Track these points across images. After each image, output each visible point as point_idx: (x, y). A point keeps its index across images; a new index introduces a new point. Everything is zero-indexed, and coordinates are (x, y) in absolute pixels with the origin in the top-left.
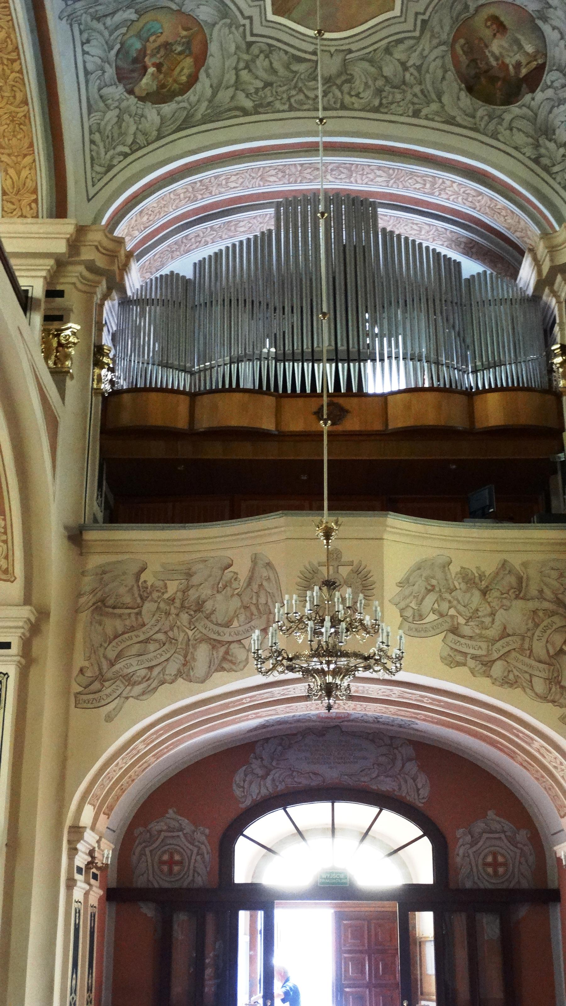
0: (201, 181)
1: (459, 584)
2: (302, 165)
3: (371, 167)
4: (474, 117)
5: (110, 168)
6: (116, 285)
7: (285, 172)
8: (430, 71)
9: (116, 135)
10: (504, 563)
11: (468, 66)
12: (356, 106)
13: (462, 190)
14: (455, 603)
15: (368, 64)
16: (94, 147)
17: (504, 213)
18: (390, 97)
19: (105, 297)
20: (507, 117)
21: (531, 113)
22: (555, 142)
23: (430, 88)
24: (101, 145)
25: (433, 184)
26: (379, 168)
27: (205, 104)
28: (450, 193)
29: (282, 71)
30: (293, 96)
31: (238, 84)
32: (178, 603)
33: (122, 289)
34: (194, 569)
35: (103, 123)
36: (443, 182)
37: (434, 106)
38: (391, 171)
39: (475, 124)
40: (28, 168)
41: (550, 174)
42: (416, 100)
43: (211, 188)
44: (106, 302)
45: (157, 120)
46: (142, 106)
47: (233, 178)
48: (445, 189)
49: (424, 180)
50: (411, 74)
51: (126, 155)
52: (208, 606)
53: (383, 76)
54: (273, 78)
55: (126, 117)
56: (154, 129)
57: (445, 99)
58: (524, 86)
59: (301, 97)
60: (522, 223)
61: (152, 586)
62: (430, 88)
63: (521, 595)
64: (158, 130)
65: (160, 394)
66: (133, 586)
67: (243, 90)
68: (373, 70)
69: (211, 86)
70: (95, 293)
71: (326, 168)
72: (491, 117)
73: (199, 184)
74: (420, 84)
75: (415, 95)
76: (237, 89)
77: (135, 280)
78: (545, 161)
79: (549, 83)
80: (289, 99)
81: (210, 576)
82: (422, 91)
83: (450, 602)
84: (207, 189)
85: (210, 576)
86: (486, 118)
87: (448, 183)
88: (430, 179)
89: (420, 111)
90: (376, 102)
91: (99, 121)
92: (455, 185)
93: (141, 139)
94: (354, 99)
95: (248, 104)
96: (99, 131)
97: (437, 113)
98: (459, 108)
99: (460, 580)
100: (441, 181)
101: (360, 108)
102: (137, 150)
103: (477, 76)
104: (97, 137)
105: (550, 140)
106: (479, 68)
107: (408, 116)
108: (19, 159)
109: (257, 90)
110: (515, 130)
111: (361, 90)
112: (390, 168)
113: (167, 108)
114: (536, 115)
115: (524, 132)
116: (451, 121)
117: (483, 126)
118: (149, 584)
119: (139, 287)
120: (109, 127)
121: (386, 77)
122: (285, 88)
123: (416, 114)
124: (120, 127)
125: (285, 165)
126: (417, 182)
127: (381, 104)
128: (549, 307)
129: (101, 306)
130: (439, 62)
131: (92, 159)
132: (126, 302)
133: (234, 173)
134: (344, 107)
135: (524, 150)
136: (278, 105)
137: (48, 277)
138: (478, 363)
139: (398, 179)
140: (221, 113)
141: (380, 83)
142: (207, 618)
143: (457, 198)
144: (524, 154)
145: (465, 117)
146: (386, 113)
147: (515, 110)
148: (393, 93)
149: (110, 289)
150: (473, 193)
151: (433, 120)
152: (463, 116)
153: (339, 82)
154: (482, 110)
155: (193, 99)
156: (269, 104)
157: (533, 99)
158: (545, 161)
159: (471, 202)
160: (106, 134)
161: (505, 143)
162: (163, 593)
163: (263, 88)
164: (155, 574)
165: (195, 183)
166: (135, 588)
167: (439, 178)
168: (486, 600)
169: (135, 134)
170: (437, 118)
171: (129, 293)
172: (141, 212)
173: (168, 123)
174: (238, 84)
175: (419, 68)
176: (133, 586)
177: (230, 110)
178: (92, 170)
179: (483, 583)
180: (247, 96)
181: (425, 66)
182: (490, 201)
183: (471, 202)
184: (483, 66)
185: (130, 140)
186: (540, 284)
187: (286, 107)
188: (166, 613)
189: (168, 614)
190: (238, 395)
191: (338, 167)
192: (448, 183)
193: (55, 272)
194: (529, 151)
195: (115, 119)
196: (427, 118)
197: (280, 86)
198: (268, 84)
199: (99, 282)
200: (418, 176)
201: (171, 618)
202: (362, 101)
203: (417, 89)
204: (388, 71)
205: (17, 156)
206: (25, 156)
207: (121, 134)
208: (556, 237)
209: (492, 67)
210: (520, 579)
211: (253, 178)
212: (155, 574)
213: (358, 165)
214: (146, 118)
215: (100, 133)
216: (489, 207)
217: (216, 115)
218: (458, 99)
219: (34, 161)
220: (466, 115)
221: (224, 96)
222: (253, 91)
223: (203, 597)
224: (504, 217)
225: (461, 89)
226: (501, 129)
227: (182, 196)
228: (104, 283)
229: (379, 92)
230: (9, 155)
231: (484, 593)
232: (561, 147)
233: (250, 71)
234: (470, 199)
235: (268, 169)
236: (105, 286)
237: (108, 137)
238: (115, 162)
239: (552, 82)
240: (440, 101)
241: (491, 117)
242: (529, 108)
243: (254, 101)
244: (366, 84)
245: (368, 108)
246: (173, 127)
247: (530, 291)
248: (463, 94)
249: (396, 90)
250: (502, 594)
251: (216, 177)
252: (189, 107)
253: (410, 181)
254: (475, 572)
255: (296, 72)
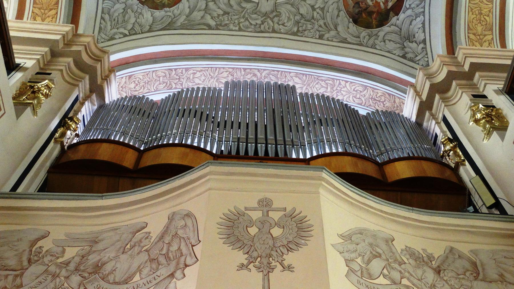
0: (176, 69)
1: (408, 259)
2: (245, 69)
3: (292, 74)
4: (359, 37)
5: (112, 39)
6: (97, 90)
7: (233, 76)
8: (330, 10)
9: (120, 20)
10: (452, 249)
11: (354, 7)
12: (282, 31)
13: (353, 88)
14: (407, 274)
15: (290, 6)
16: (102, 21)
17: (383, 99)
18: (304, 28)
19: (87, 98)
20: (381, 34)
21: (397, 28)
22: (416, 42)
23: (330, 23)
24: (109, 23)
25: (332, 88)
26: (297, 75)
27: (185, 17)
28: (344, 93)
29: (235, 7)
30: (241, 22)
31: (207, 9)
32: (72, 266)
33: (101, 96)
34: (100, 238)
35: (112, 10)
36: (340, 84)
37: (333, 33)
38: (304, 77)
39: (360, 41)
40: (51, 17)
41: (415, 62)
42: (320, 29)
43: (182, 80)
44: (86, 103)
45: (151, 19)
46: (142, 8)
47: (198, 74)
48: (341, 90)
49: (327, 84)
50: (318, 13)
51: (125, 35)
52: (108, 267)
53: (300, 13)
54: (228, 10)
55: (129, 11)
56: (148, 24)
57: (340, 28)
58: (391, 13)
59: (247, 23)
60: (397, 100)
61: (47, 251)
62: (330, 23)
63: (481, 277)
64: (150, 26)
65: (112, 146)
66: (24, 251)
67: (210, 14)
68: (293, 10)
69: (189, 7)
70: (78, 86)
71: (261, 74)
72: (370, 36)
73: (174, 72)
74: (324, 19)
75: (320, 26)
76: (206, 13)
77: (113, 93)
78: (409, 56)
79: (408, 6)
80: (239, 24)
81: (118, 241)
82: (325, 24)
83: (400, 272)
84: (179, 79)
85: (118, 241)
86: (367, 37)
87: (343, 83)
88: (330, 82)
89: (323, 35)
90: (295, 29)
91: (110, 8)
92: (348, 84)
93: (137, 28)
94: (281, 27)
95: (212, 23)
96: (109, 14)
97: (335, 37)
98: (349, 33)
99: (408, 256)
100: (338, 81)
101: (285, 32)
102: (134, 34)
103: (360, 13)
104: (107, 17)
105: (412, 42)
106: (361, 8)
107: (316, 38)
108: (46, 11)
109: (219, 15)
110: (387, 41)
111: (285, 21)
112: (303, 74)
113: (159, 14)
114: (401, 29)
115: (393, 41)
116: (344, 41)
117: (365, 41)
118: (44, 250)
119: (116, 100)
120: (116, 14)
121: (302, 15)
122: (236, 17)
123: (321, 37)
124: (124, 17)
125: (233, 68)
126: (322, 87)
127: (298, 31)
128: (429, 132)
129: (82, 104)
130: (335, 5)
131: (100, 28)
132: (102, 106)
133: (199, 69)
134: (274, 31)
135: (394, 52)
136: (231, 27)
137: (41, 62)
138: (383, 149)
139: (309, 85)
140: (193, 25)
141: (298, 17)
142: (103, 279)
143: (349, 97)
144: (395, 54)
145: (354, 38)
146: (302, 36)
147: (386, 29)
148: (306, 24)
149: (91, 91)
150: (360, 89)
151: (332, 41)
152: (352, 38)
153: (271, 16)
154: (364, 33)
155: (177, 12)
156: (226, 25)
157: (398, 19)
158: (409, 56)
159: (359, 98)
160: (114, 17)
161: (381, 50)
162: (58, 258)
163: (223, 15)
164: (54, 241)
165: (171, 70)
166: (26, 254)
167: (337, 79)
168: (442, 278)
169: (134, 23)
170: (334, 40)
171: (107, 101)
172: (130, 77)
173: (156, 24)
174: (207, 9)
175: (322, 9)
176: (24, 251)
177: (199, 24)
178: (99, 34)
179: (433, 263)
180: (212, 18)
181: (326, 8)
182: (373, 91)
183: (359, 98)
184: (363, 5)
185: (130, 27)
186: (421, 113)
187: (237, 28)
188: (53, 276)
189: (55, 276)
190: (179, 149)
191: (269, 75)
192: (343, 83)
193: (48, 62)
194: (397, 52)
195: (122, 11)
196: (328, 40)
197: (234, 15)
198: (226, 13)
199: (83, 78)
200: (322, 80)
201: (58, 280)
202: (286, 28)
203: (321, 22)
204: (302, 11)
205: (45, 10)
206: (51, 10)
207: (124, 21)
208: (430, 69)
209: (370, 6)
210: (474, 264)
211: (212, 78)
212: (54, 241)
213: (282, 71)
214: (143, 16)
215: (109, 15)
216: (372, 98)
217: (190, 25)
218: (348, 28)
219: (57, 13)
220: (354, 37)
221: (197, 15)
222: (216, 15)
223: (105, 259)
224: (383, 102)
225: (349, 22)
226: (377, 42)
227: (161, 78)
228: (87, 82)
229: (297, 23)
230: (40, 9)
231: (438, 271)
232: (420, 43)
233: (215, 3)
234: (358, 96)
235: (222, 70)
236: (88, 86)
237: (114, 20)
238: (117, 37)
239: (410, 5)
240: (336, 30)
241: (370, 36)
242: (395, 25)
243: (216, 22)
244: (289, 18)
245: (290, 33)
246: (161, 27)
247: (414, 119)
248: (351, 25)
249: (308, 23)
250: (459, 275)
251: (187, 70)
252: (173, 17)
253: (317, 86)
254: (421, 252)
255: (244, 8)
